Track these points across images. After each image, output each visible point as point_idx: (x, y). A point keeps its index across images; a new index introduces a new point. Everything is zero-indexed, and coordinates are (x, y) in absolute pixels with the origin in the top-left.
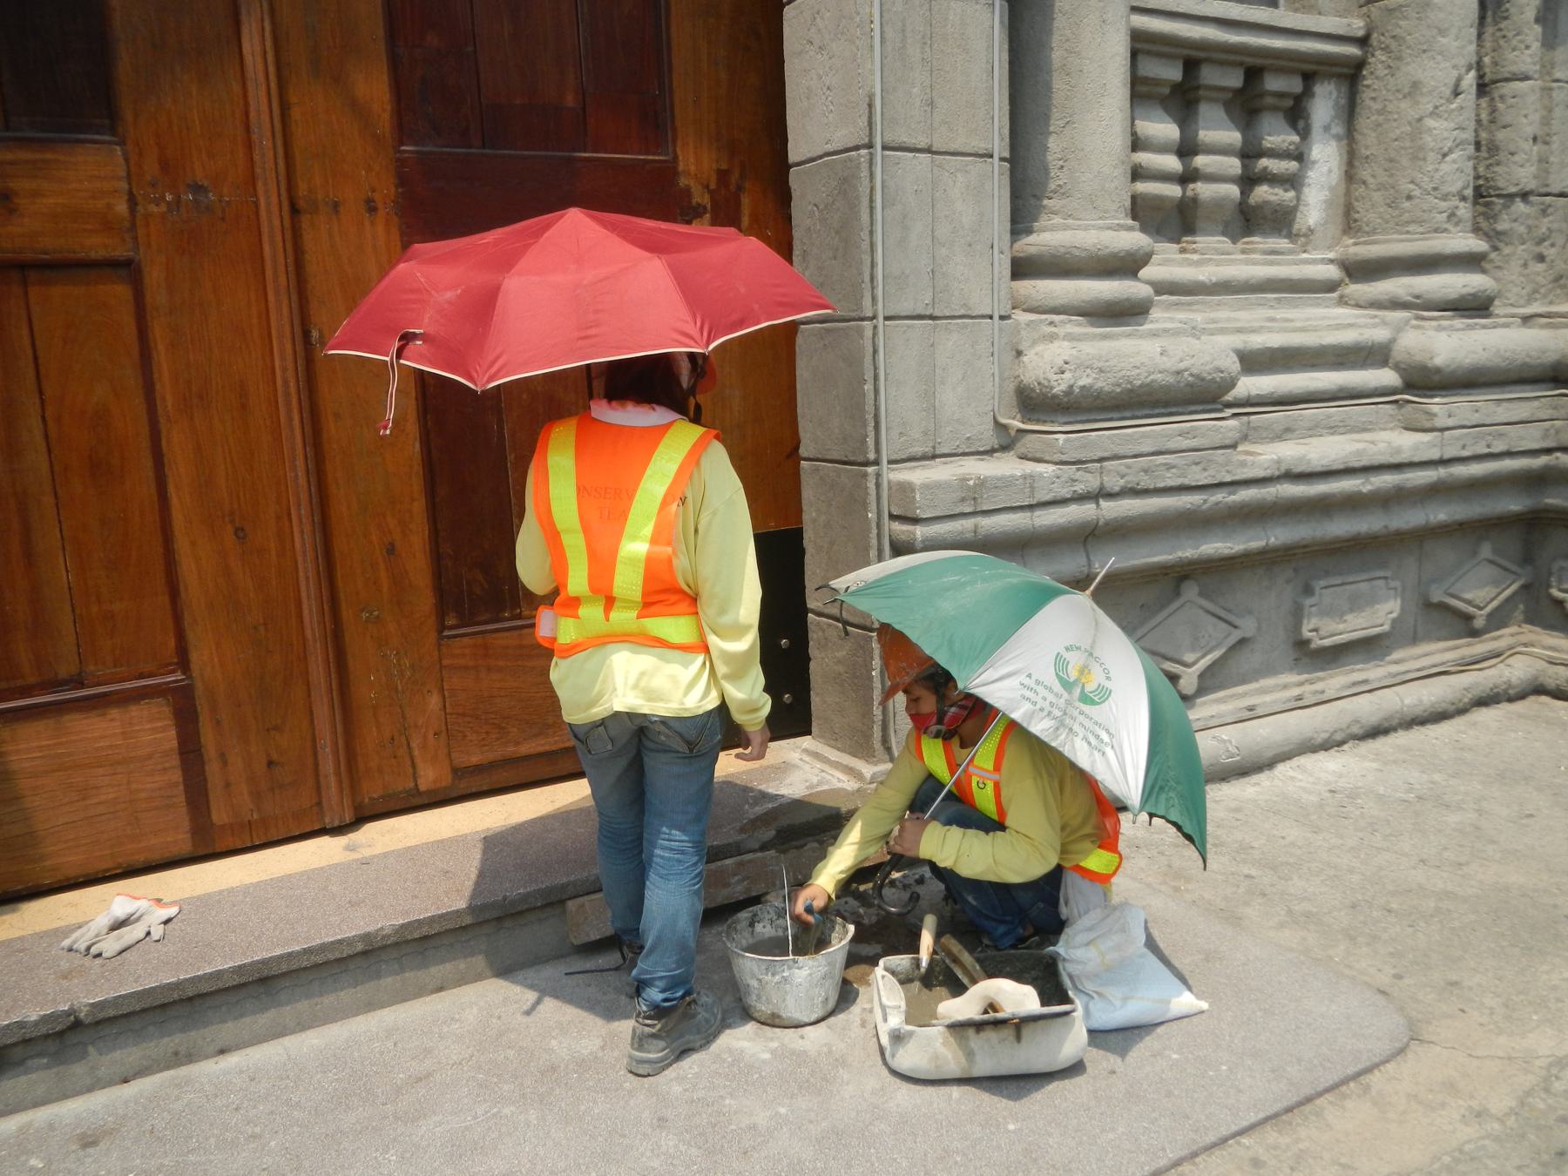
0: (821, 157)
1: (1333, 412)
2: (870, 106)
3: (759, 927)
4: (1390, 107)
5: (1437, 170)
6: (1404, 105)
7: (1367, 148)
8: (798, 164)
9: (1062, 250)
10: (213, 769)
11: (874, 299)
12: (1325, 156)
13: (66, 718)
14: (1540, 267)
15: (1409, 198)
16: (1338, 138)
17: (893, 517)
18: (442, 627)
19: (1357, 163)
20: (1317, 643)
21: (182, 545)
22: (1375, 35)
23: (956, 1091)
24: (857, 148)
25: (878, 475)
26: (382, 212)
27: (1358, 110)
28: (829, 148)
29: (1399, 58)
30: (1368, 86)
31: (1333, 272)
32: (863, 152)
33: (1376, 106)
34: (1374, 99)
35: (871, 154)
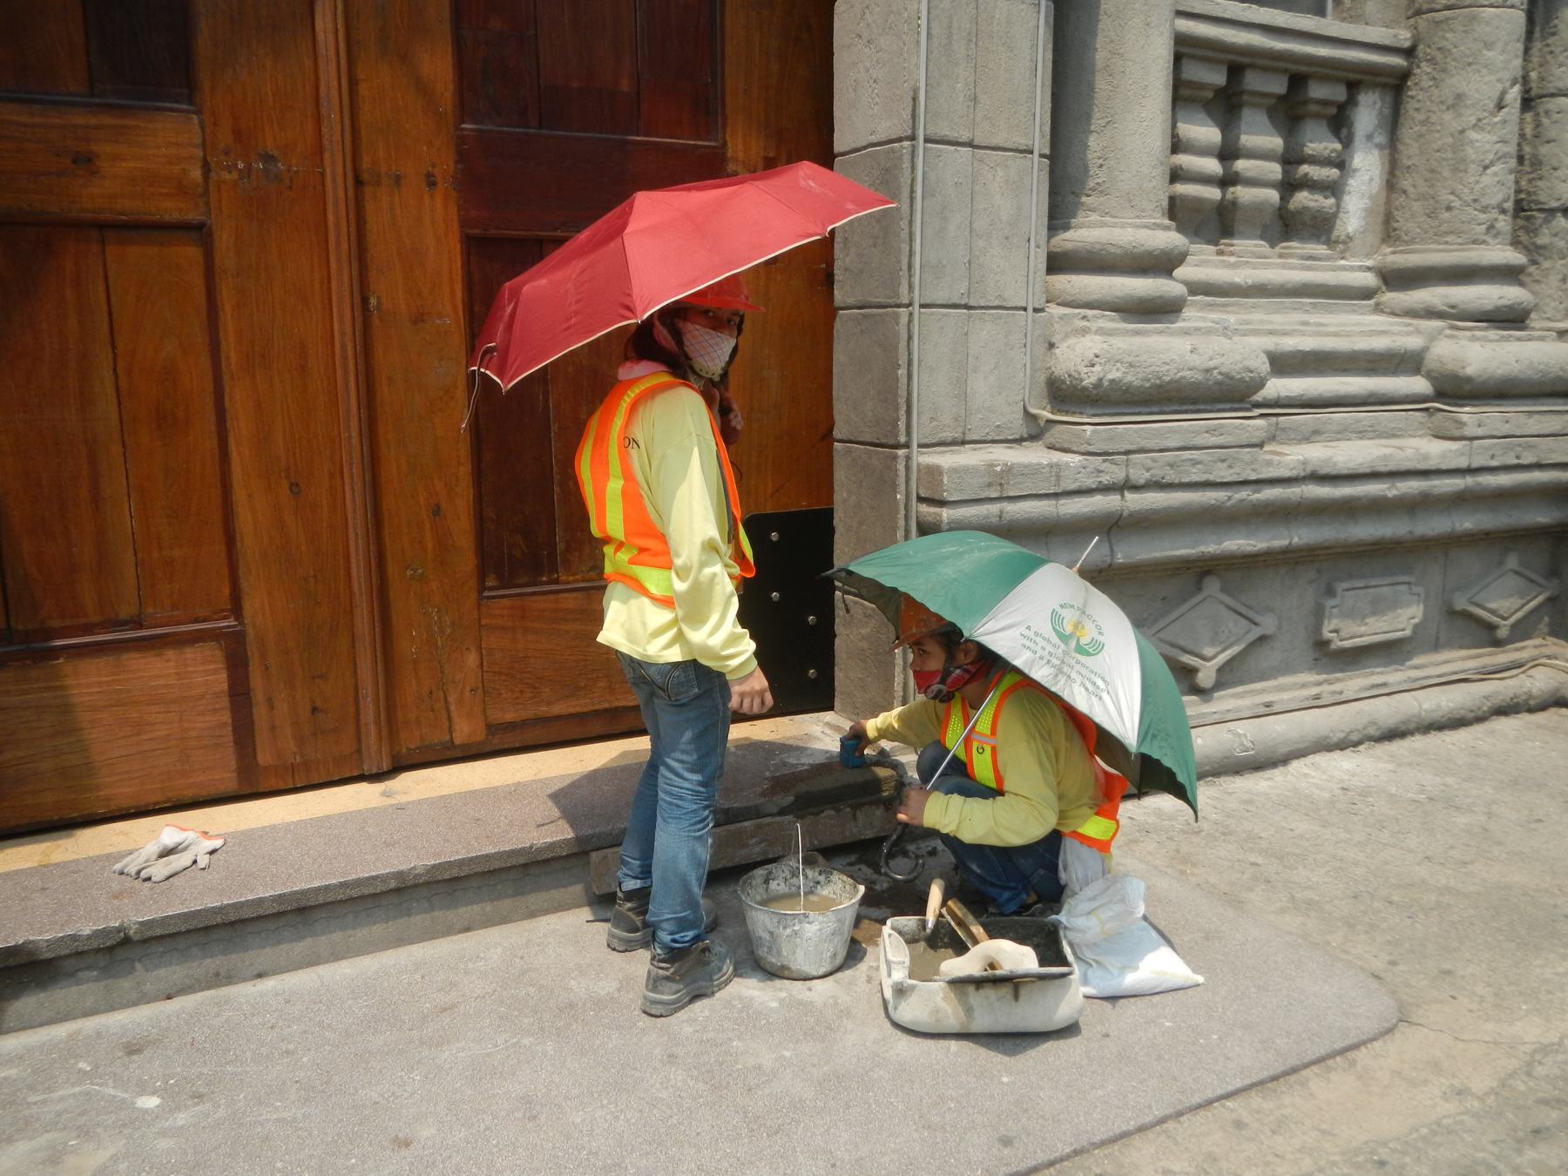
0: (865, 148)
1: (1363, 417)
2: (915, 99)
3: (773, 885)
4: (1434, 118)
5: (1478, 182)
6: (1447, 116)
7: (1409, 157)
8: (843, 154)
9: (1098, 247)
10: (260, 712)
11: (911, 286)
12: (1367, 165)
13: (125, 656)
15: (1449, 208)
16: (1380, 147)
17: (921, 499)
18: (482, 588)
19: (1398, 173)
20: (1337, 644)
21: (239, 495)
22: (1421, 47)
23: (954, 1045)
24: (900, 140)
25: (908, 458)
26: (440, 186)
27: (1402, 120)
28: (874, 139)
29: (1444, 70)
30: (1412, 97)
31: (1370, 280)
32: (906, 144)
33: (1420, 117)
34: (1417, 110)
35: (913, 146)
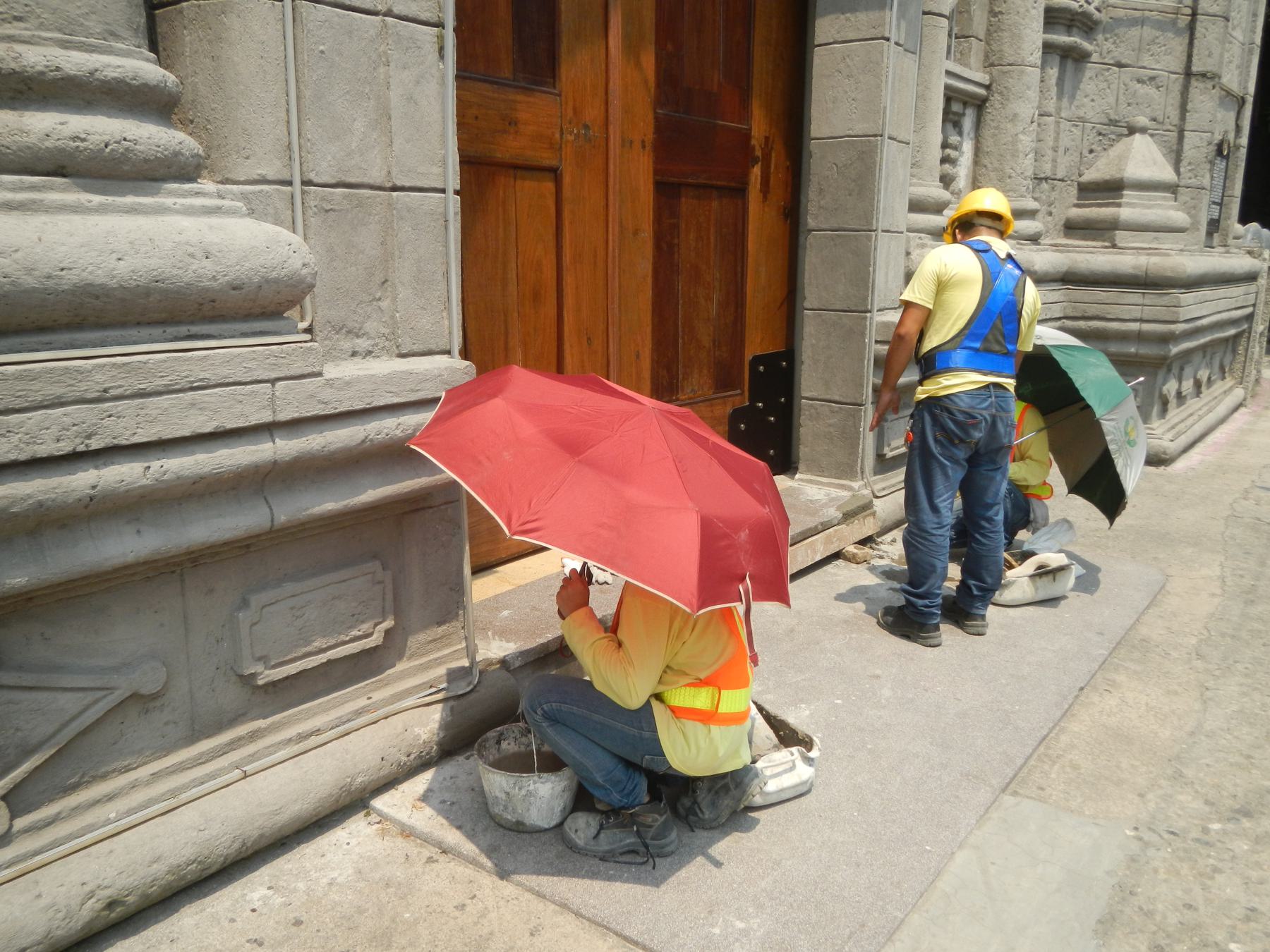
4: (1002, 126)
5: (1023, 163)
6: (1009, 126)
7: (988, 147)
9: (923, 198)
12: (968, 147)
14: (1050, 218)
15: (1010, 177)
16: (971, 139)
17: (877, 342)
19: (981, 155)
21: (567, 346)
22: (994, 85)
23: (1030, 608)
24: (875, 136)
27: (982, 125)
28: (851, 132)
29: (1008, 100)
30: (989, 113)
32: (879, 138)
33: (993, 124)
34: (993, 120)
